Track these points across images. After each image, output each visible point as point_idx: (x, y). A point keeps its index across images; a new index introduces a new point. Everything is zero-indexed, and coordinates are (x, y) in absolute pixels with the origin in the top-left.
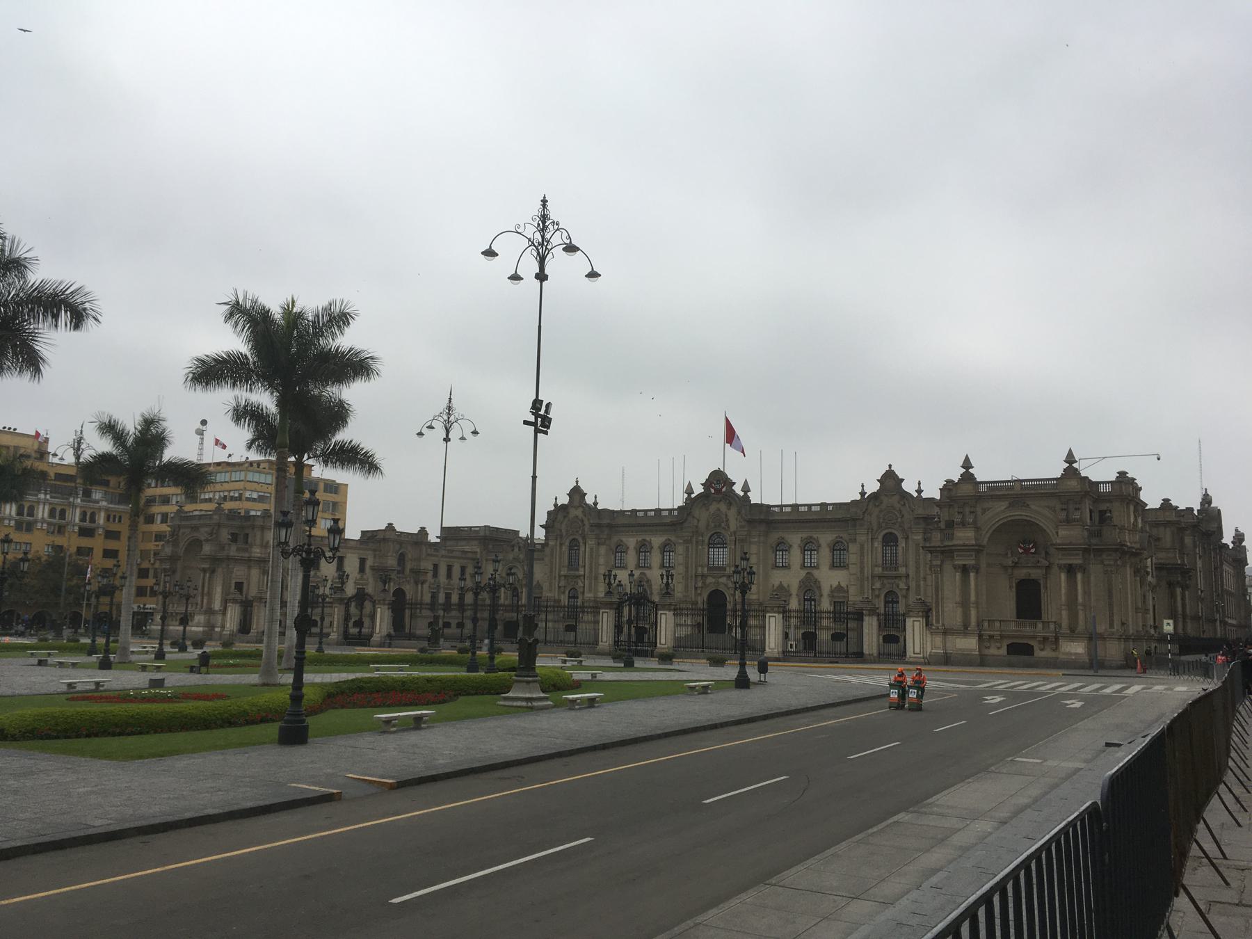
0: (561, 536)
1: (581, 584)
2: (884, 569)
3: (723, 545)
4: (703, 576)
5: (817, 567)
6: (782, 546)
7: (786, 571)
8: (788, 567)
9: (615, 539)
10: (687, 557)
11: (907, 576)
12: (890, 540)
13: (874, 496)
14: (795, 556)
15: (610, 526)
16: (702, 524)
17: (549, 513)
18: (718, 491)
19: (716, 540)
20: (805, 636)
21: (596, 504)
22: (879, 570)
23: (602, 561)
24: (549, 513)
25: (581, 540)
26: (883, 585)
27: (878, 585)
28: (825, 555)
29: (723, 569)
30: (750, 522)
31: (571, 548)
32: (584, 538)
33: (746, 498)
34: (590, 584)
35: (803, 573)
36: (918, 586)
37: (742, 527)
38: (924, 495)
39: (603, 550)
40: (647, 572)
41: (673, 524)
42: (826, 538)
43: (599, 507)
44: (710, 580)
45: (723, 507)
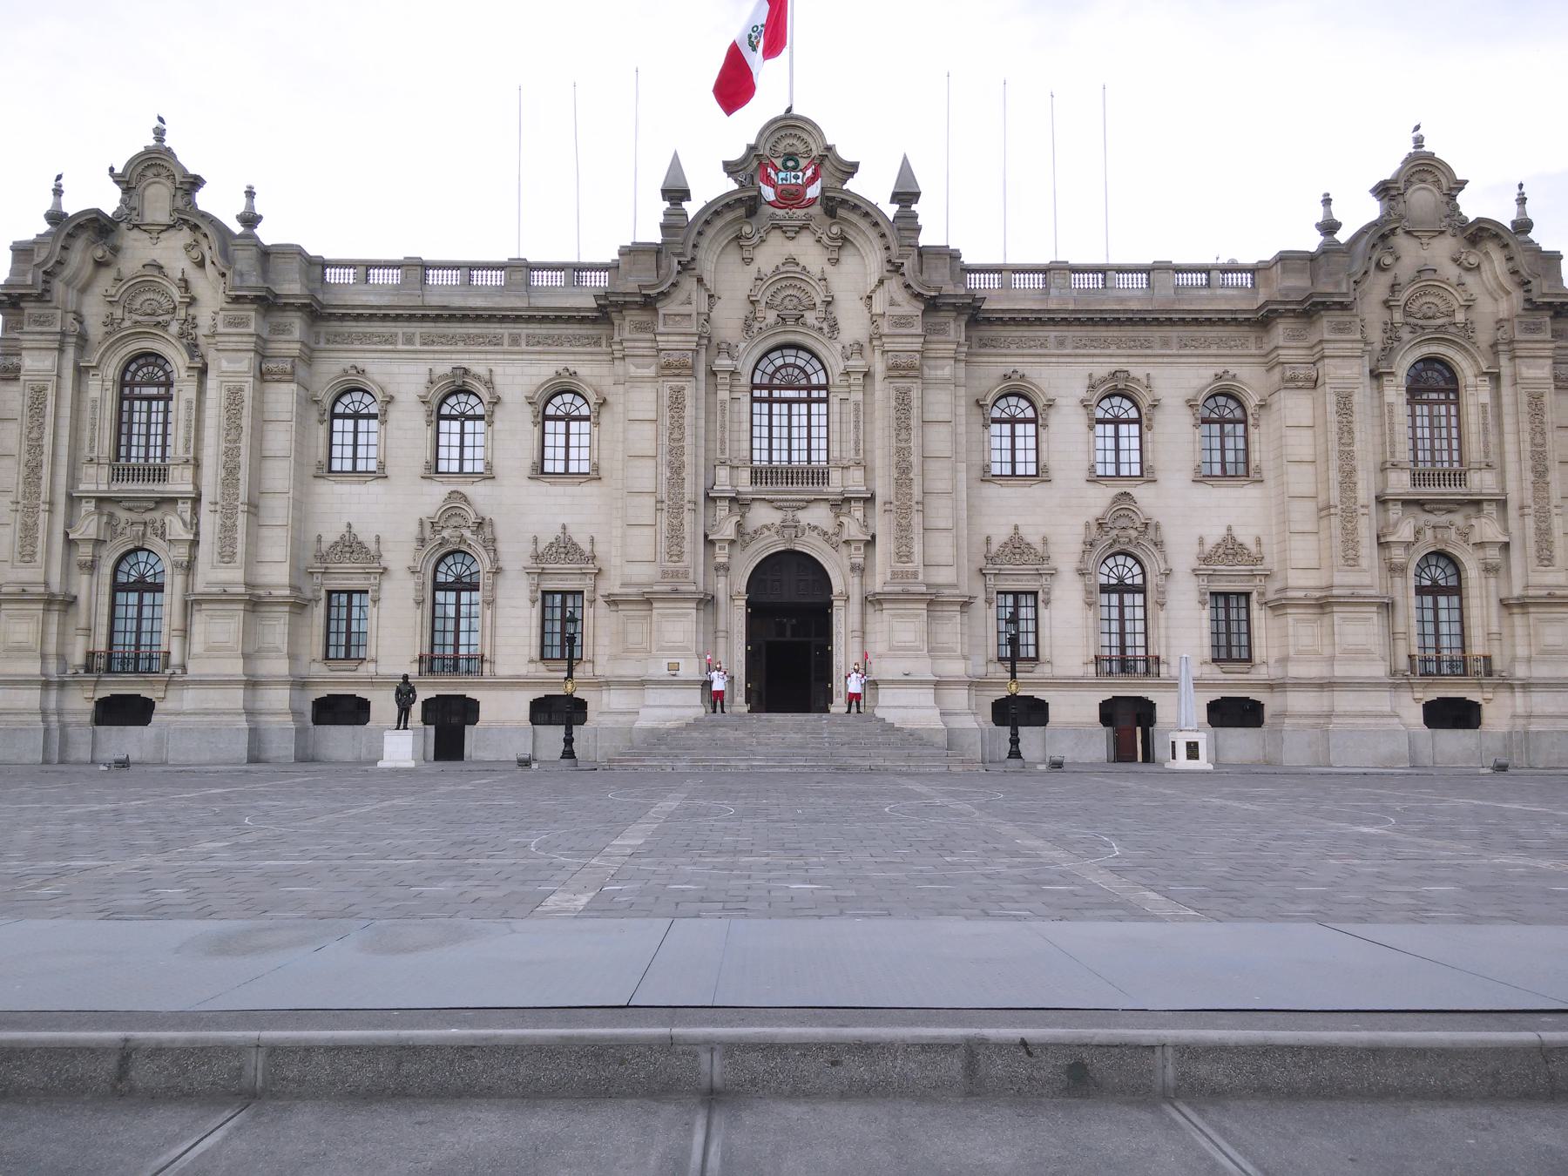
0: (82, 341)
1: (176, 527)
2: (1417, 478)
3: (815, 394)
4: (738, 502)
5: (1146, 475)
6: (1020, 402)
7: (1037, 490)
8: (1041, 474)
9: (331, 367)
10: (677, 425)
11: (1502, 504)
12: (1434, 381)
13: (1379, 235)
14: (1071, 439)
15: (317, 313)
16: (728, 319)
17: (22, 252)
18: (791, 197)
19: (788, 374)
20: (1109, 712)
21: (250, 220)
22: (1400, 483)
23: (280, 440)
24: (22, 252)
25: (178, 360)
26: (1418, 532)
27: (1405, 532)
28: (1177, 438)
29: (821, 476)
30: (932, 305)
31: (126, 391)
32: (193, 349)
33: (908, 223)
34: (227, 530)
35: (1099, 499)
36: (1544, 534)
37: (902, 321)
38: (1543, 237)
39: (283, 397)
40: (477, 492)
41: (606, 312)
42: (1176, 379)
43: (267, 234)
44: (762, 515)
45: (809, 252)
